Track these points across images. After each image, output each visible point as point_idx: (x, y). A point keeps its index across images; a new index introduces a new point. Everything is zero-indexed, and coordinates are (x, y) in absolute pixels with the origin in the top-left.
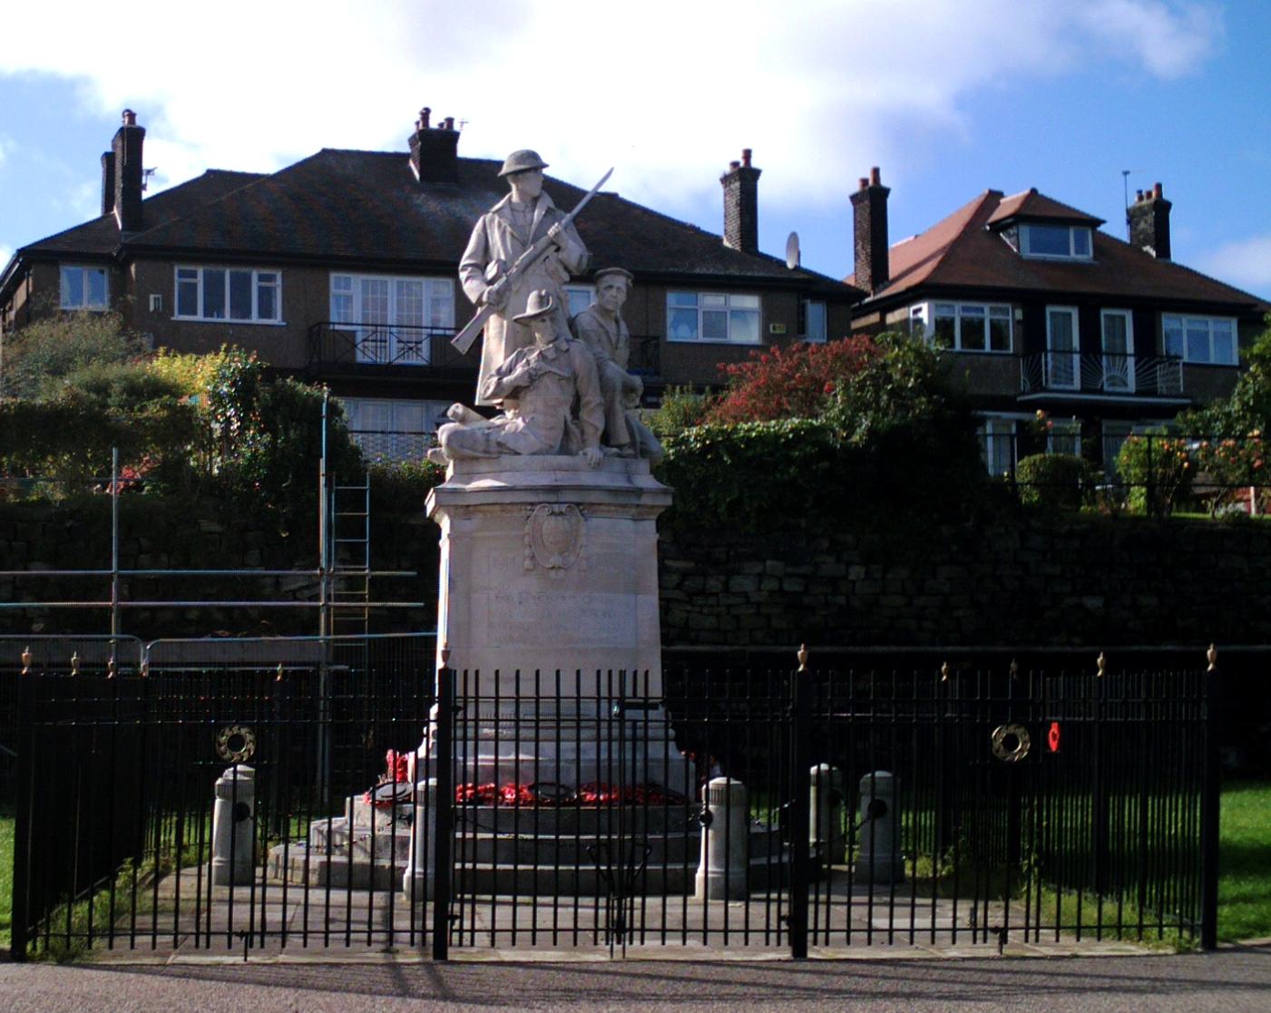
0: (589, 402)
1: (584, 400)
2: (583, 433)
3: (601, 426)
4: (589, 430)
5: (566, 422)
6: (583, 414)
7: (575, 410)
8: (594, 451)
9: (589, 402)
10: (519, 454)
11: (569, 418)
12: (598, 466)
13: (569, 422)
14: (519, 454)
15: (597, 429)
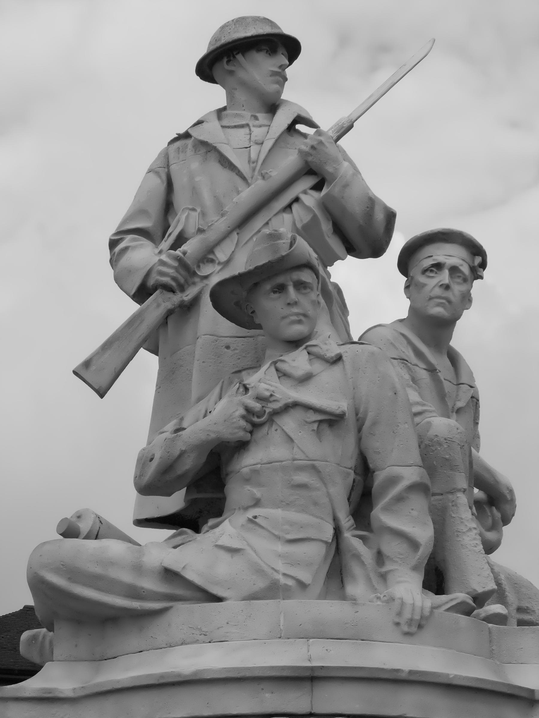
0: (393, 481)
1: (380, 477)
2: (380, 558)
3: (424, 533)
4: (392, 547)
5: (338, 532)
6: (381, 515)
7: (363, 500)
8: (408, 588)
9: (393, 481)
10: (219, 599)
11: (346, 522)
12: (415, 627)
13: (347, 535)
14: (219, 599)
15: (414, 544)
